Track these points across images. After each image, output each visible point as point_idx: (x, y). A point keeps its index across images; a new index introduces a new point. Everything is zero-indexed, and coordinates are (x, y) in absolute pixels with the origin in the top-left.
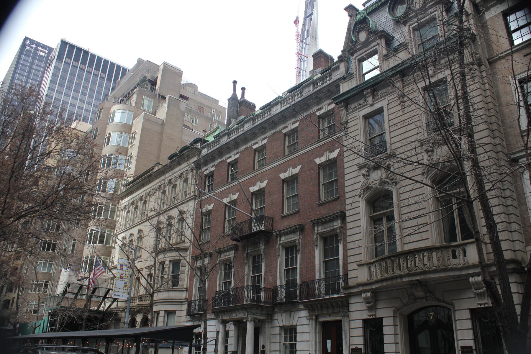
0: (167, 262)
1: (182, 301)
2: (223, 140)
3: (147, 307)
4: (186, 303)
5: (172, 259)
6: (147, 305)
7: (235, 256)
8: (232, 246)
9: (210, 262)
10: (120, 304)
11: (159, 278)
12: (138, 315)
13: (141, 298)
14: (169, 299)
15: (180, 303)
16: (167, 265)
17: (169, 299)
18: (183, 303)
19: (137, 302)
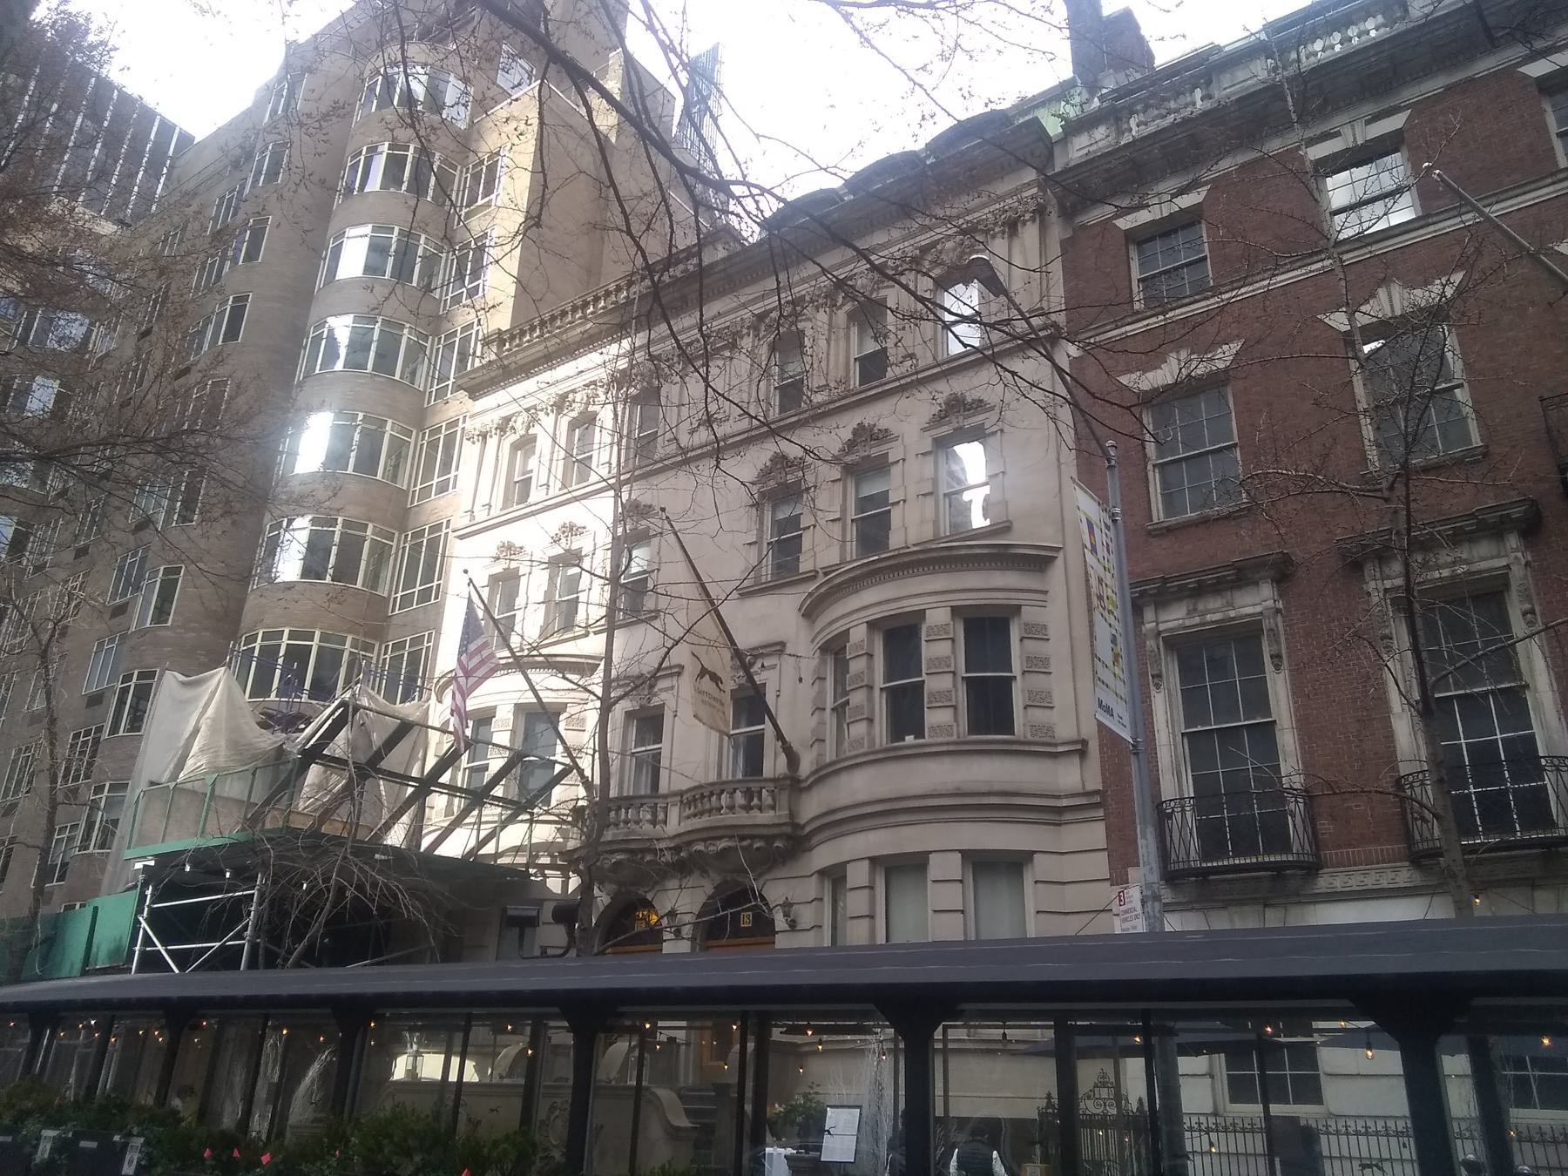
0: (859, 634)
1: (1065, 802)
2: (1241, 75)
3: (769, 839)
4: (1100, 813)
5: (876, 613)
6: (765, 832)
7: (1527, 564)
8: (1517, 512)
9: (1280, 605)
10: (544, 833)
11: (877, 692)
12: (673, 883)
13: (696, 798)
14: (989, 794)
15: (1053, 812)
16: (858, 646)
17: (989, 794)
18: (1068, 816)
19: (675, 823)
